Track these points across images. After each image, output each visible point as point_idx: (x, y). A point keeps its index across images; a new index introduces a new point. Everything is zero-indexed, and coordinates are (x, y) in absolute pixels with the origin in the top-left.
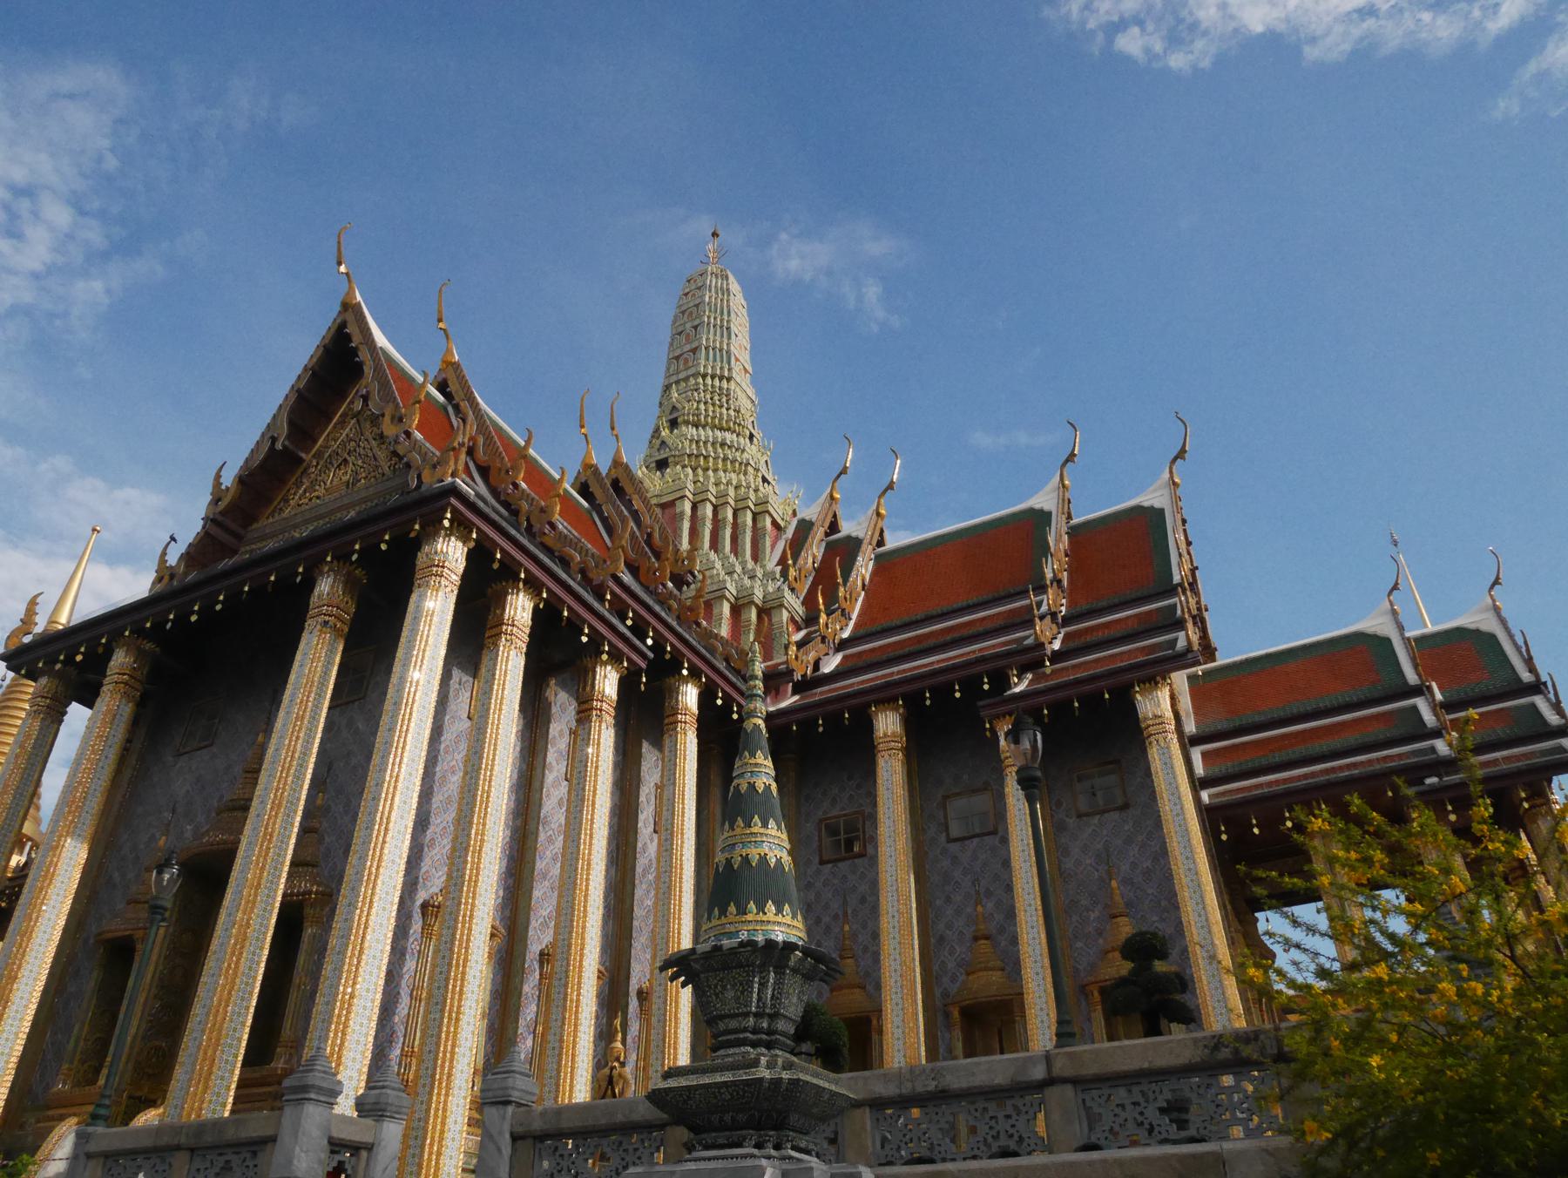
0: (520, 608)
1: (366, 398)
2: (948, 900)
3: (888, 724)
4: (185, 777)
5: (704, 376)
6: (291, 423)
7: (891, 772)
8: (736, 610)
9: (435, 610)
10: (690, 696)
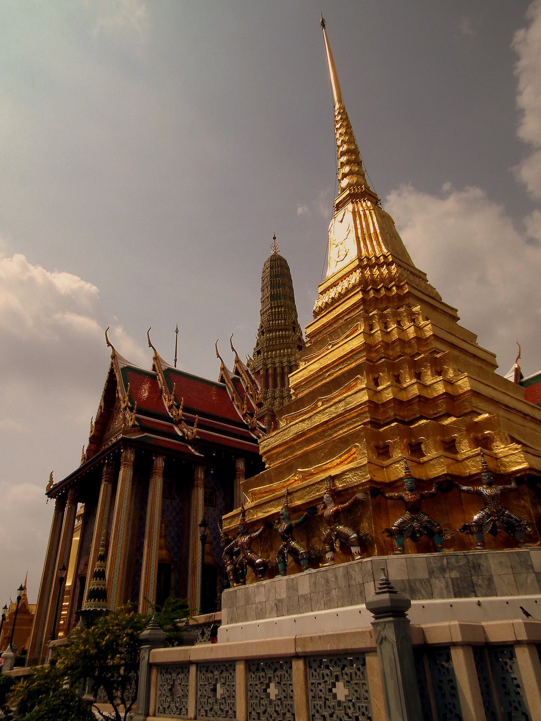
1: (118, 393)
9: (125, 475)
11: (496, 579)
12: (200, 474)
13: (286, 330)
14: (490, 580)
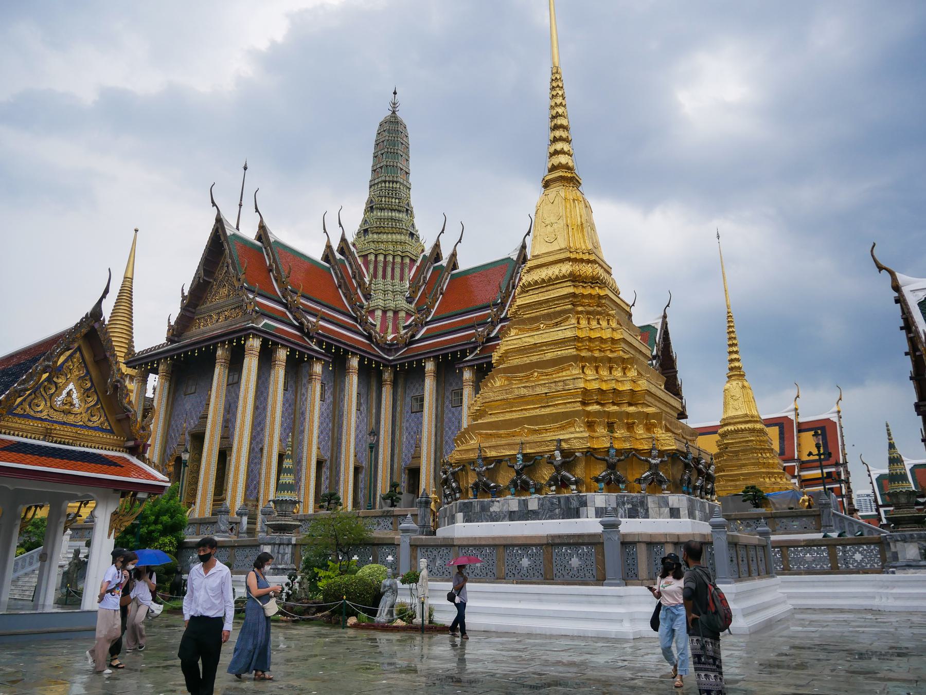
0: (282, 354)
2: (450, 429)
3: (430, 366)
4: (188, 403)
5: (385, 182)
6: (204, 270)
7: (429, 384)
8: (384, 312)
9: (251, 364)
10: (354, 362)
11: (650, 510)
12: (318, 368)
13: (399, 211)
14: (647, 510)
